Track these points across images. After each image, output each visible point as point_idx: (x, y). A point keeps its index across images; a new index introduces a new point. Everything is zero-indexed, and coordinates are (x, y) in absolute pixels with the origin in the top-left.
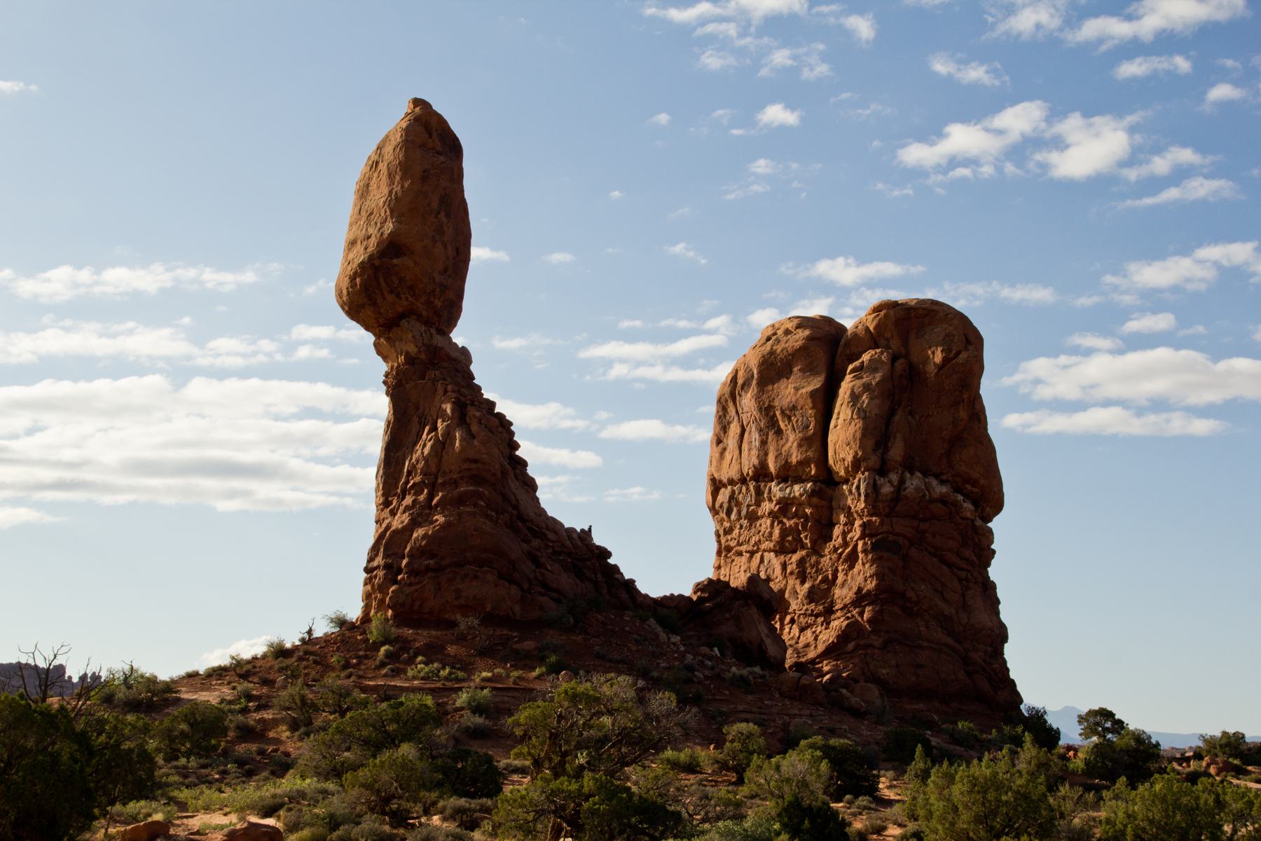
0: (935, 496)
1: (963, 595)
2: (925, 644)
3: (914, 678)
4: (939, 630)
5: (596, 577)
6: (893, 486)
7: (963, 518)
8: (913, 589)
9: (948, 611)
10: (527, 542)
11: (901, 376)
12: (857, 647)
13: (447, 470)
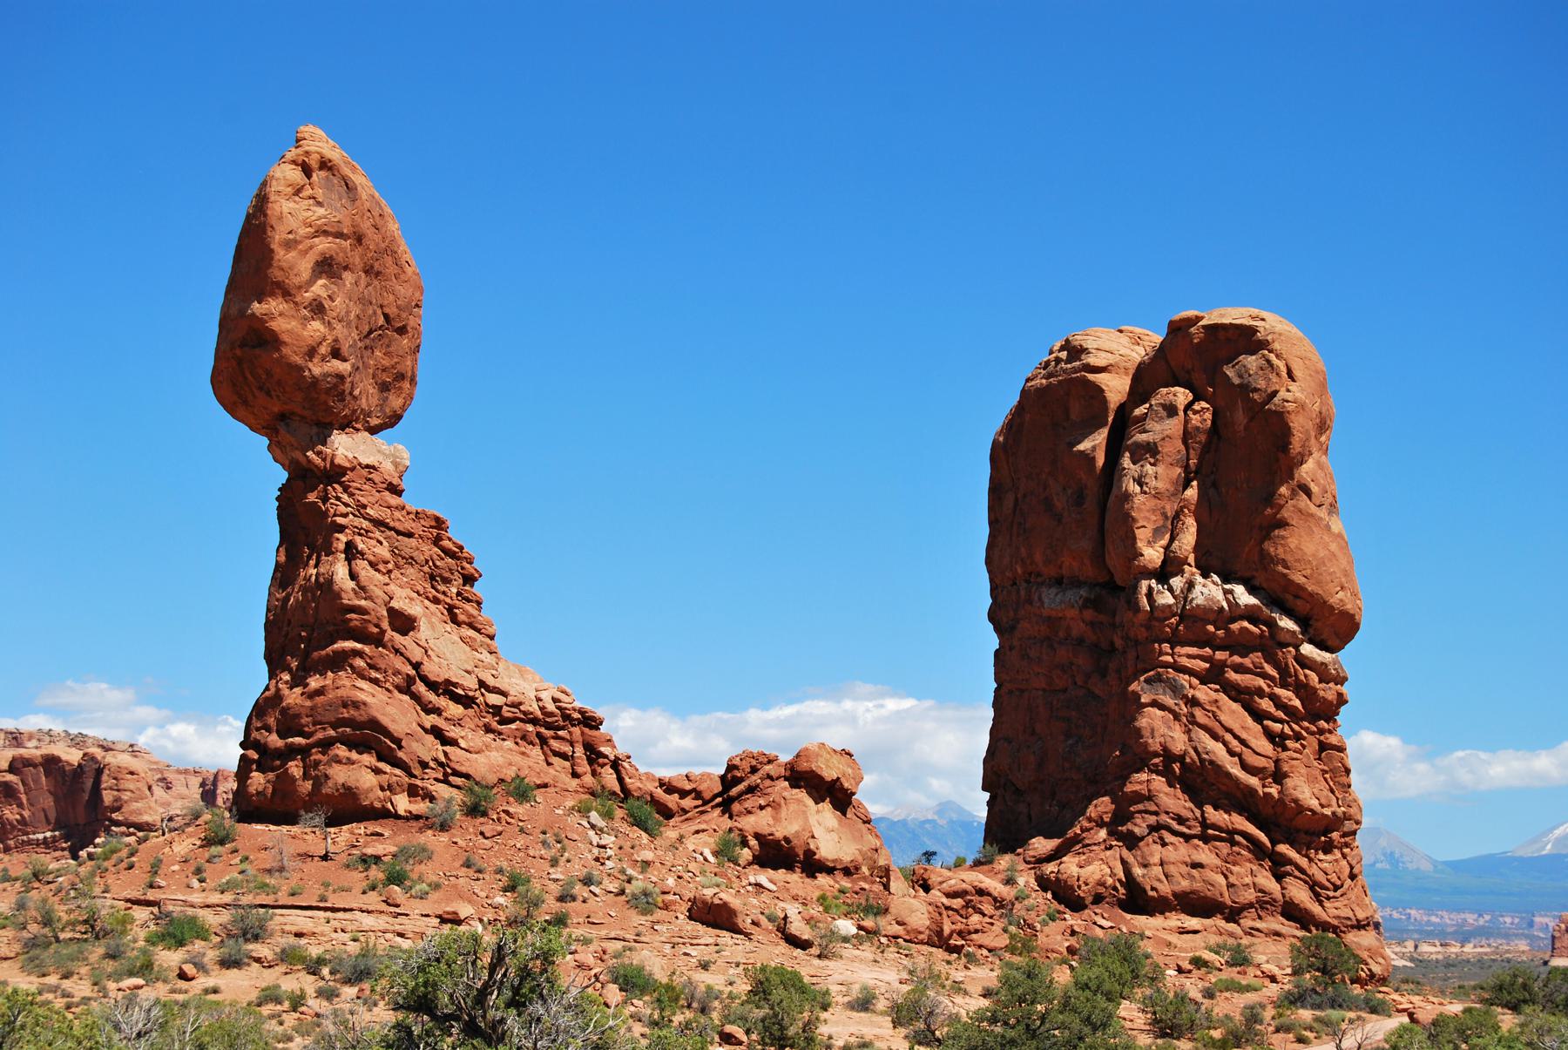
1: (1277, 762)
2: (1210, 831)
5: (574, 752)
6: (1175, 597)
8: (1195, 749)
9: (1254, 781)
10: (430, 709)
13: (325, 621)
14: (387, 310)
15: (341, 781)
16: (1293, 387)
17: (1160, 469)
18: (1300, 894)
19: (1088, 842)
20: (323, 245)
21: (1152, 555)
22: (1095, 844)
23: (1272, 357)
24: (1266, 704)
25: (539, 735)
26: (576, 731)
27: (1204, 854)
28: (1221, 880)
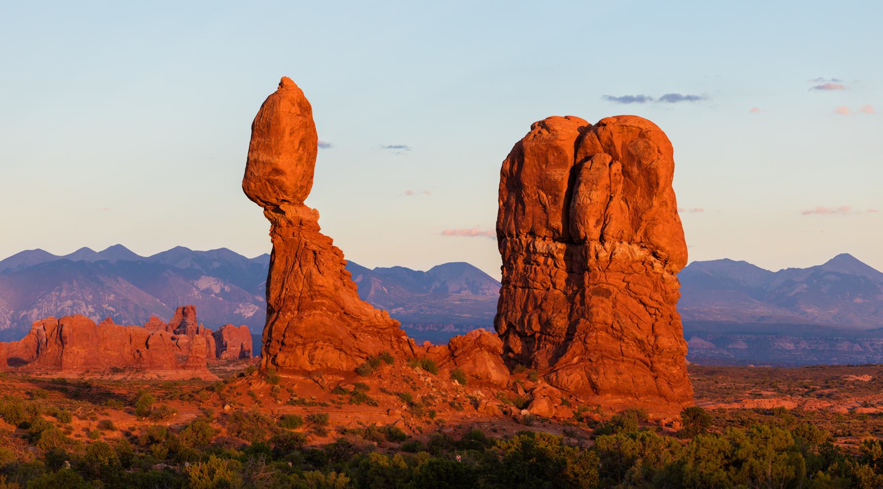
0: (636, 258)
2: (625, 359)
3: (615, 382)
4: (635, 348)
7: (654, 273)
8: (618, 322)
11: (615, 174)
12: (581, 360)
15: (321, 357)
16: (662, 157)
17: (599, 193)
18: (665, 387)
19: (569, 364)
21: (595, 233)
22: (572, 365)
23: (650, 142)
24: (646, 300)
25: (378, 332)
27: (622, 367)
28: (631, 380)
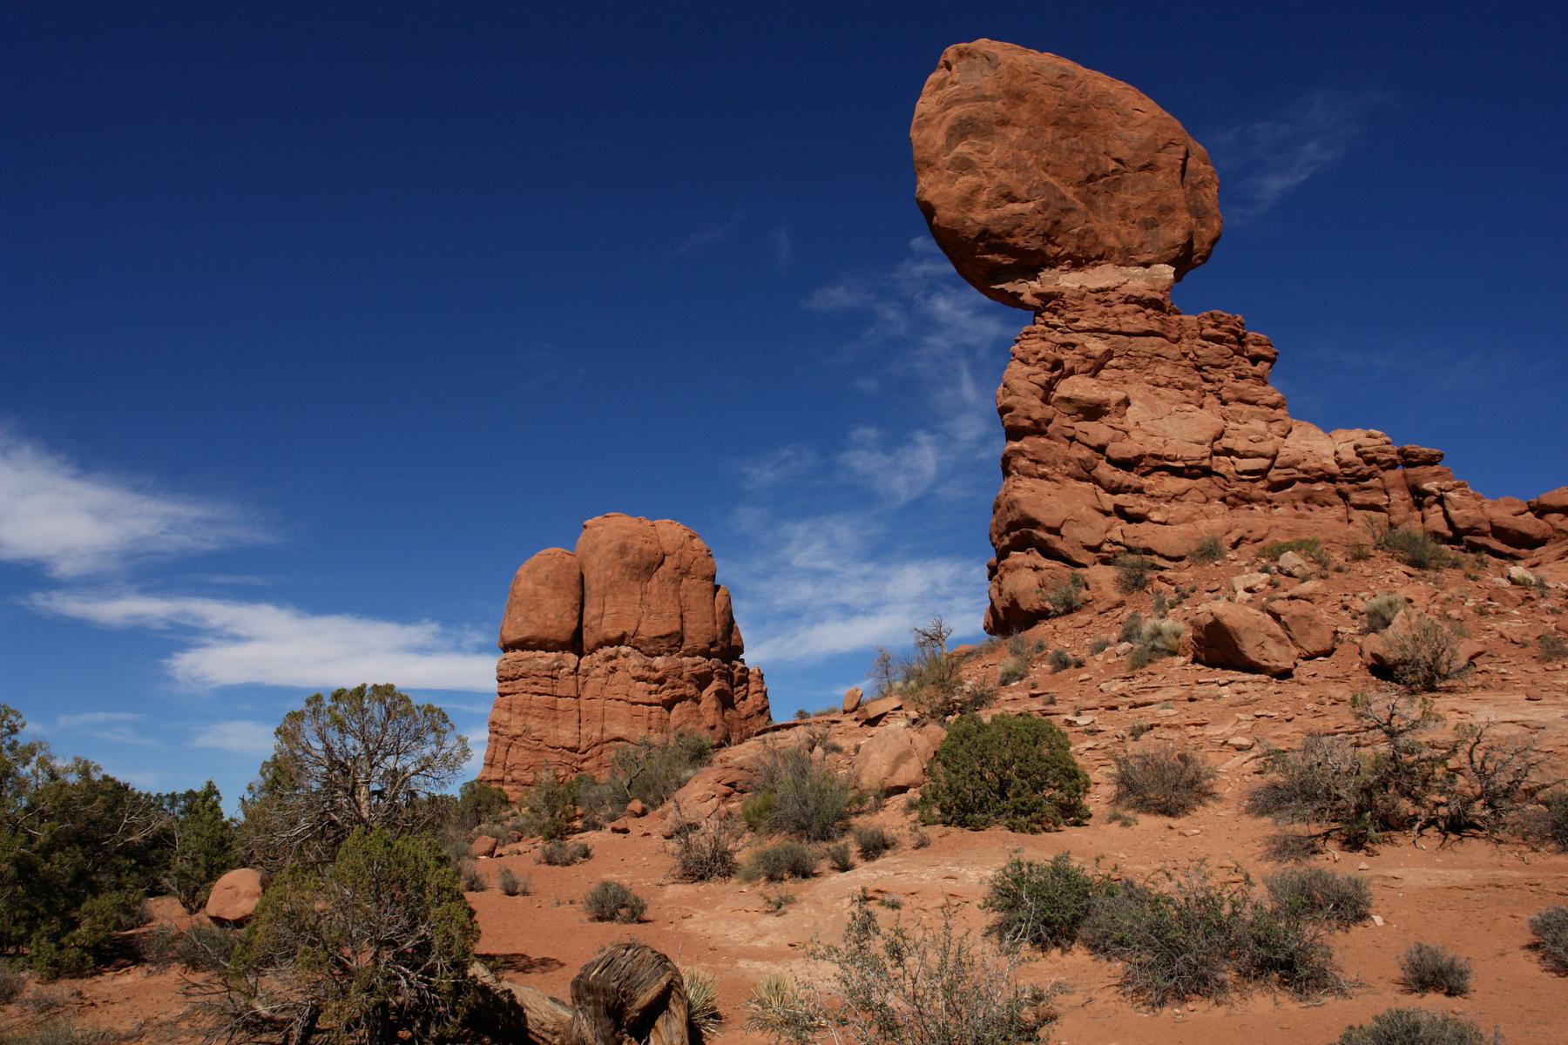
14: (1117, 155)
20: (956, 111)
26: (1393, 476)
